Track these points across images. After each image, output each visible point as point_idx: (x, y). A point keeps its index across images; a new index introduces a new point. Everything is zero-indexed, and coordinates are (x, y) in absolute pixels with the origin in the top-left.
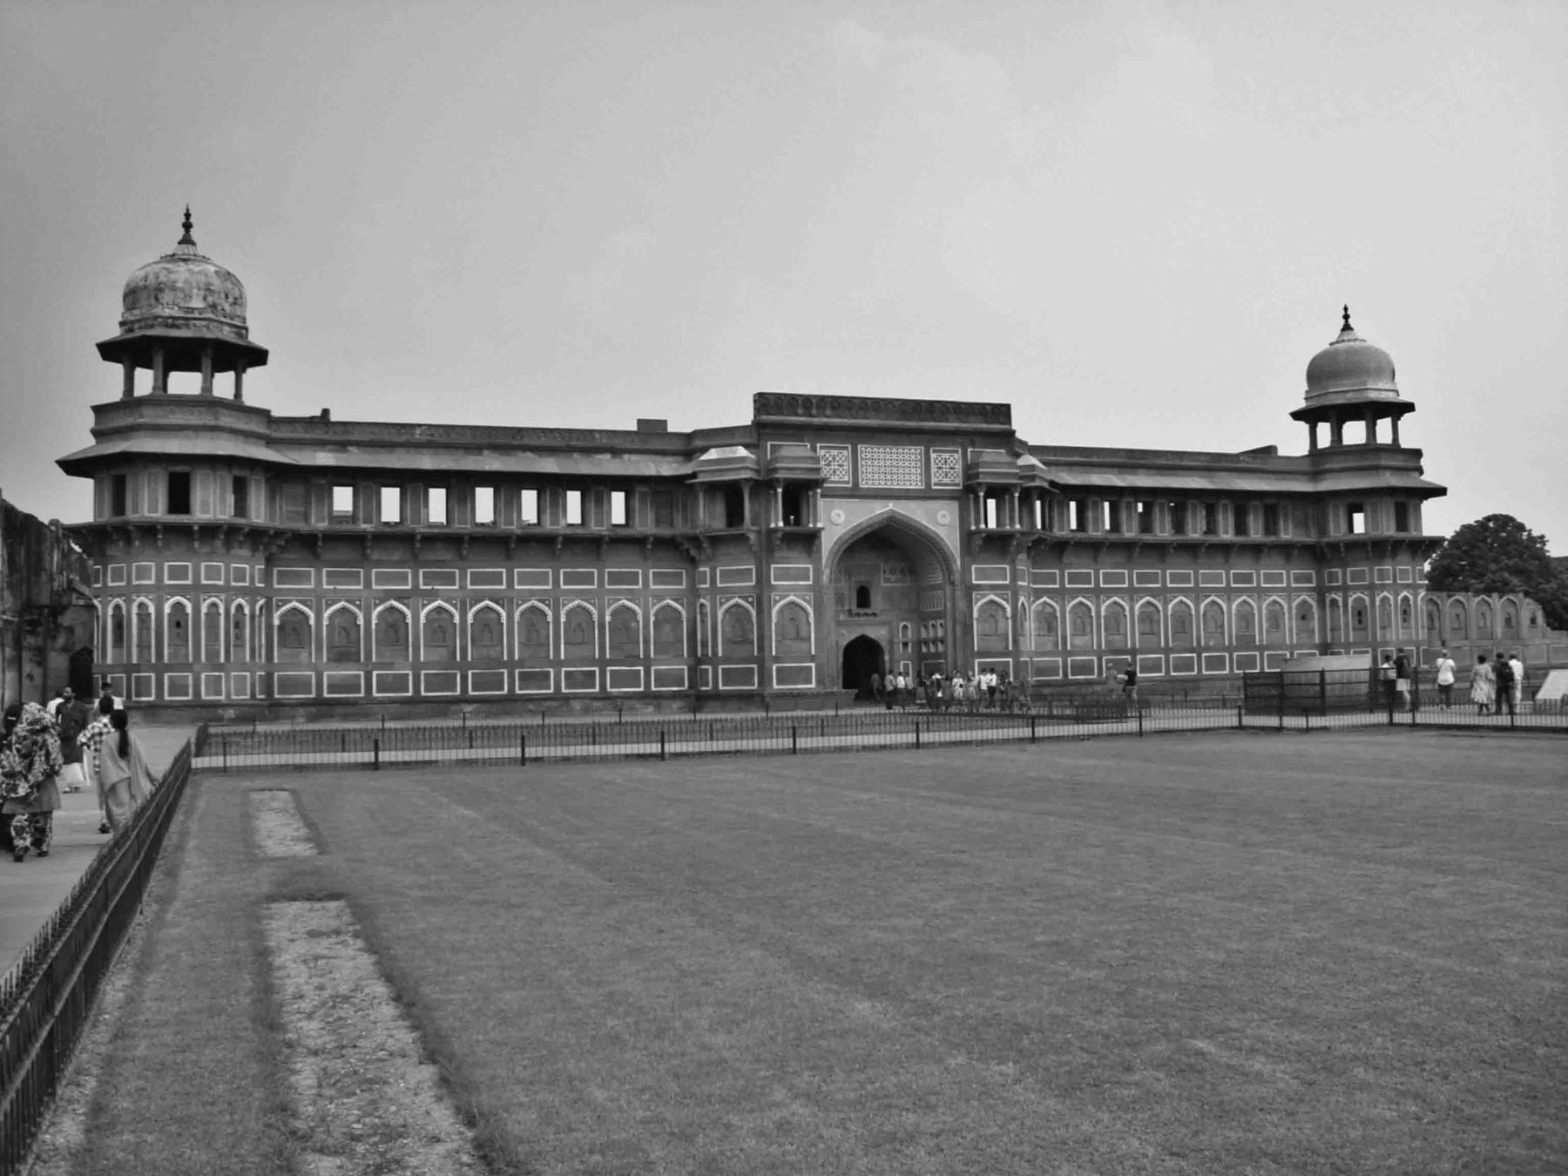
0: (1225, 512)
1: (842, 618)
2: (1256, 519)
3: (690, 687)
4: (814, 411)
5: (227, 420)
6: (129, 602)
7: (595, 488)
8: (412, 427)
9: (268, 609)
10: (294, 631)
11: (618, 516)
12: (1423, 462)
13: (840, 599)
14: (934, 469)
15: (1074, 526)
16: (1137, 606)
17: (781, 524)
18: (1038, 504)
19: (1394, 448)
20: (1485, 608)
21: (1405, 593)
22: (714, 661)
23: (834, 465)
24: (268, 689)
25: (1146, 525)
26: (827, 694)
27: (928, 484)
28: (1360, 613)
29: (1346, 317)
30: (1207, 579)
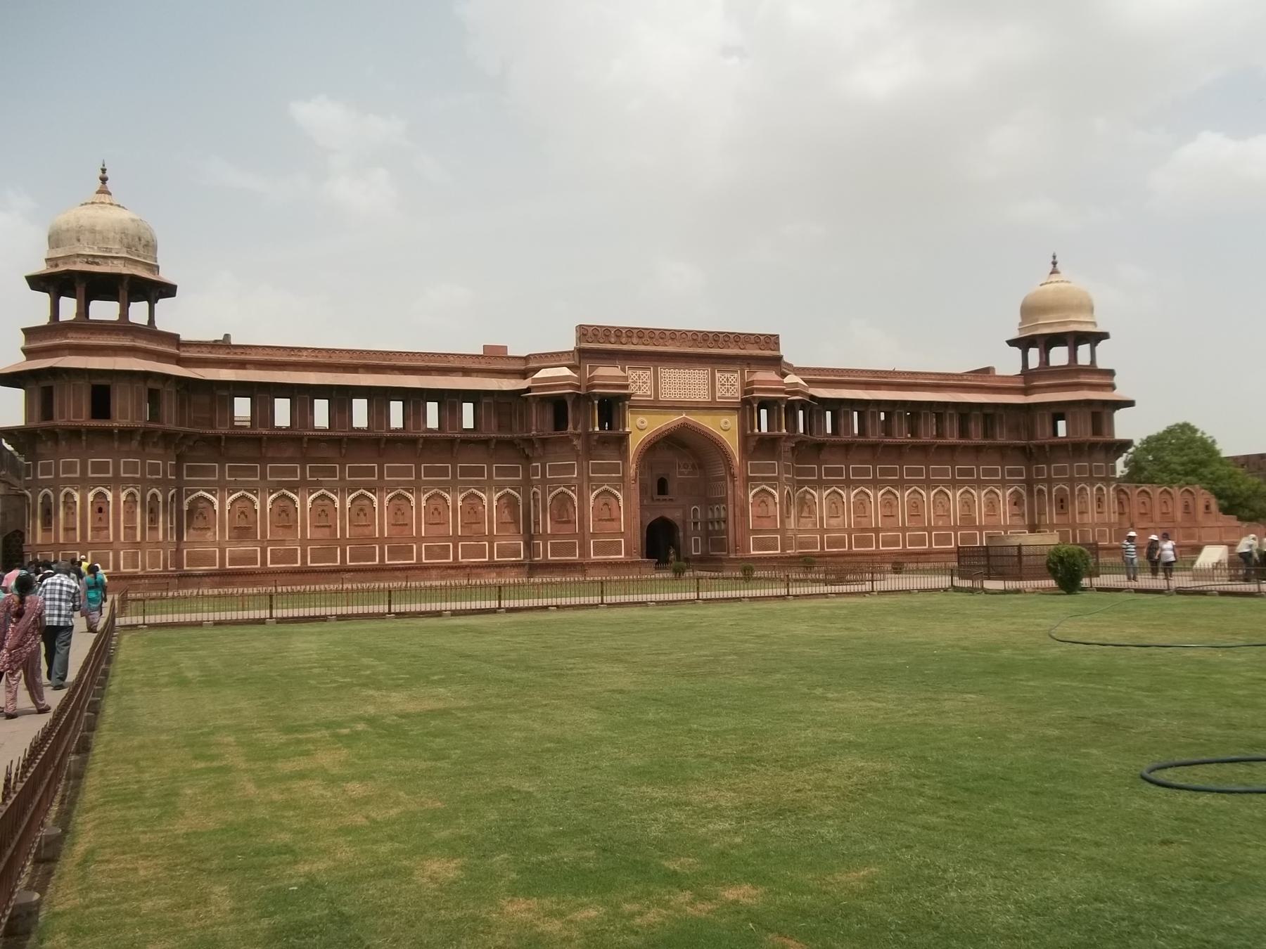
0: (951, 420)
2: (976, 425)
4: (624, 340)
8: (300, 349)
9: (179, 498)
11: (468, 421)
13: (643, 490)
14: (718, 385)
15: (829, 430)
17: (597, 429)
18: (801, 413)
19: (1092, 369)
20: (1168, 497)
24: (178, 564)
25: (888, 433)
27: (714, 397)
28: (1062, 501)
29: (1054, 264)
30: (936, 472)
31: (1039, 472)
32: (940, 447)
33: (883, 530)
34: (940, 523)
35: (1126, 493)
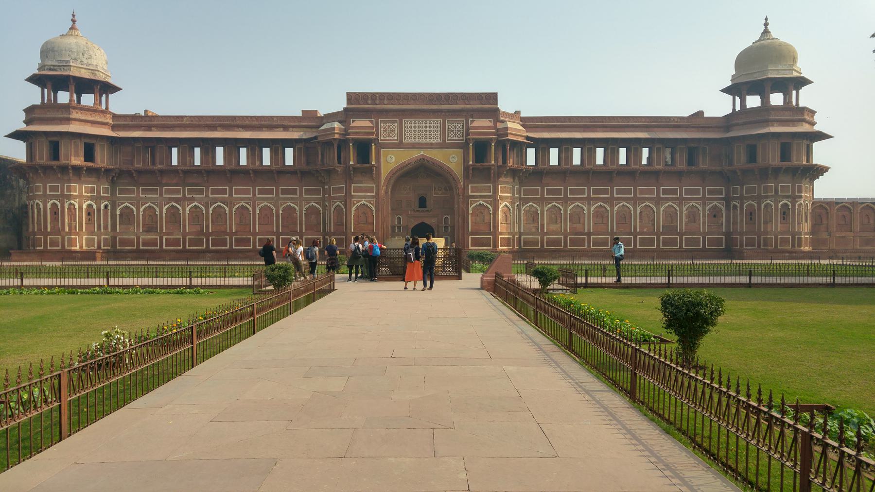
4: (377, 102)
10: (127, 217)
11: (289, 160)
16: (592, 209)
22: (331, 234)
28: (751, 214)
29: (766, 25)
33: (594, 234)
34: (645, 230)
35: (826, 209)
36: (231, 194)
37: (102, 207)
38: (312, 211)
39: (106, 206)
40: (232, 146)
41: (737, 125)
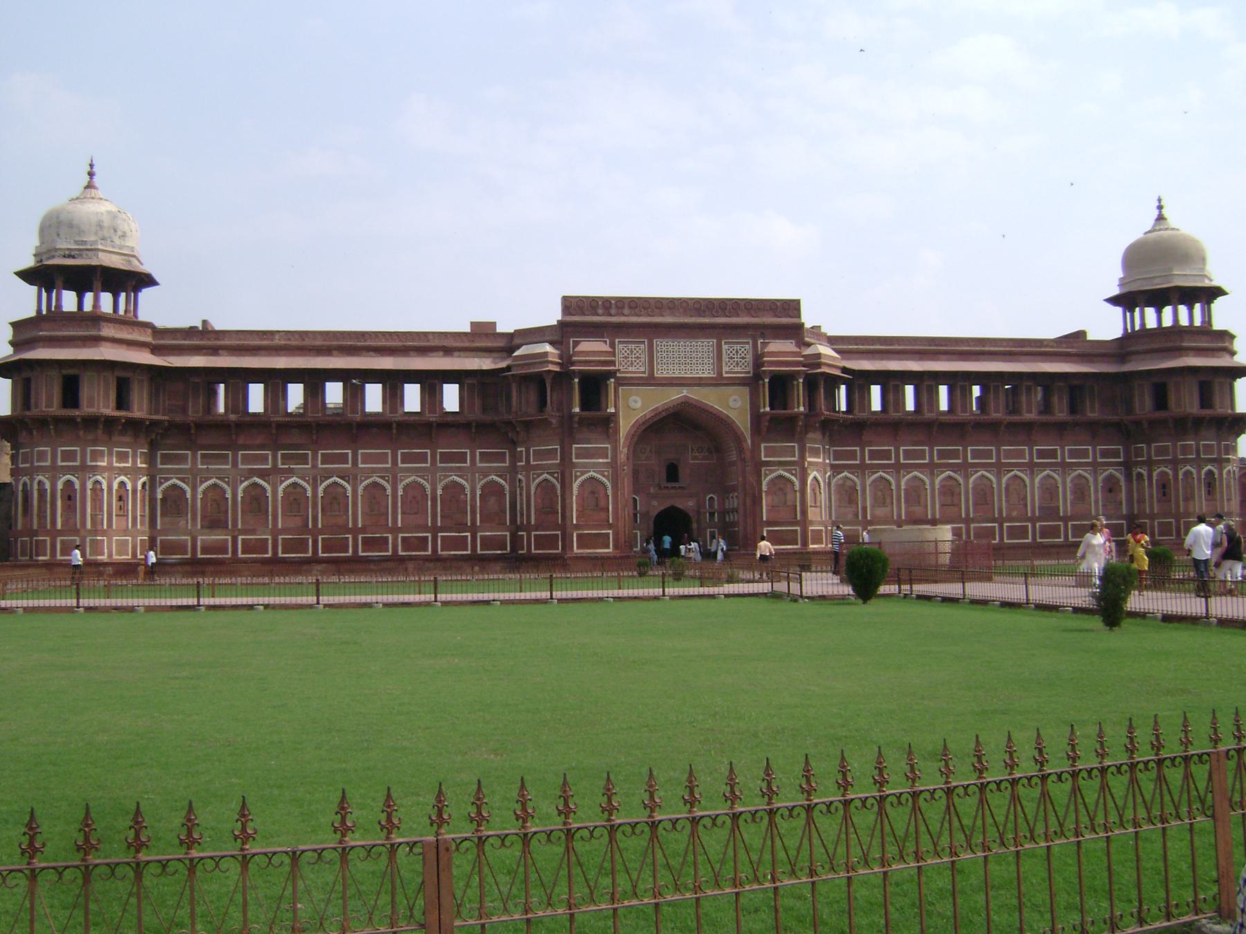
1: (652, 490)
2: (1060, 398)
3: (513, 549)
4: (613, 311)
5: (108, 331)
6: (32, 479)
7: (431, 382)
8: (272, 333)
10: (174, 503)
12: (1235, 341)
14: (725, 358)
16: (937, 481)
17: (577, 410)
21: (1209, 467)
22: (528, 528)
23: (632, 358)
26: (622, 557)
28: (1164, 486)
29: (1160, 208)
30: (1009, 454)
31: (1139, 452)
32: (1012, 425)
34: (1014, 514)
36: (355, 463)
37: (139, 488)
38: (492, 490)
39: (144, 484)
40: (354, 380)
41: (1138, 353)
